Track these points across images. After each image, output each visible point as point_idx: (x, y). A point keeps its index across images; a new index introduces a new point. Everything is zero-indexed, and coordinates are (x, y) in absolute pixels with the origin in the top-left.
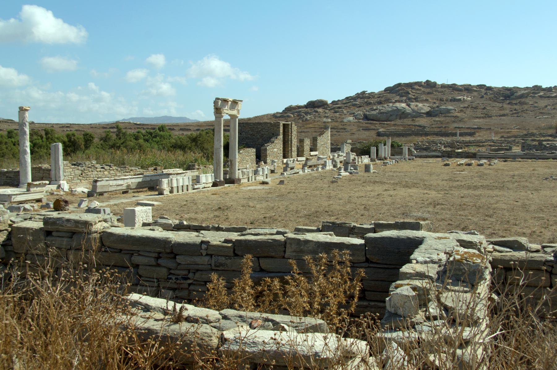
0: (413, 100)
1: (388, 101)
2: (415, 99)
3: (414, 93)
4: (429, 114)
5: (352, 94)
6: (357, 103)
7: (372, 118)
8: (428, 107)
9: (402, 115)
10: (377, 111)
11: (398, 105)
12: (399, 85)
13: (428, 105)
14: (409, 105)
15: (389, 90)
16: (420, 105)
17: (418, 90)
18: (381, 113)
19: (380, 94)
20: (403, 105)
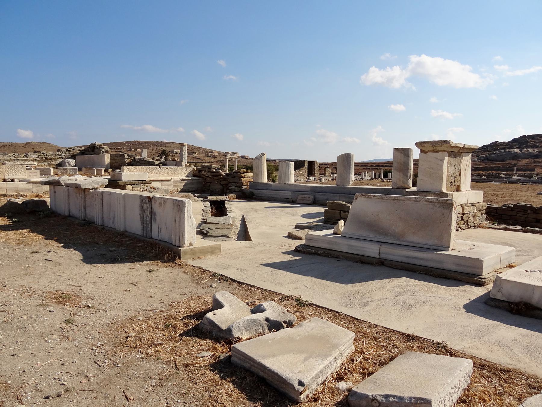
0: (529, 147)
1: (511, 147)
2: (532, 146)
3: (533, 142)
4: (536, 156)
5: (488, 143)
6: (488, 149)
7: (490, 159)
8: (537, 151)
9: (516, 157)
10: (495, 155)
11: (512, 150)
12: (524, 136)
13: (537, 150)
14: (521, 151)
15: (515, 140)
16: (531, 150)
17: (538, 139)
18: (498, 156)
19: (509, 142)
20: (517, 151)
